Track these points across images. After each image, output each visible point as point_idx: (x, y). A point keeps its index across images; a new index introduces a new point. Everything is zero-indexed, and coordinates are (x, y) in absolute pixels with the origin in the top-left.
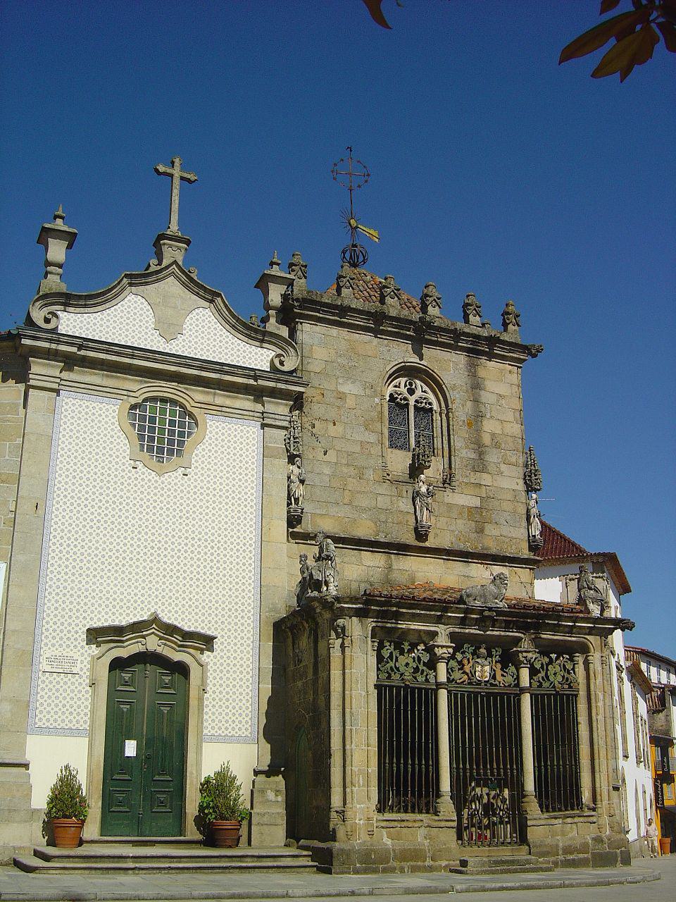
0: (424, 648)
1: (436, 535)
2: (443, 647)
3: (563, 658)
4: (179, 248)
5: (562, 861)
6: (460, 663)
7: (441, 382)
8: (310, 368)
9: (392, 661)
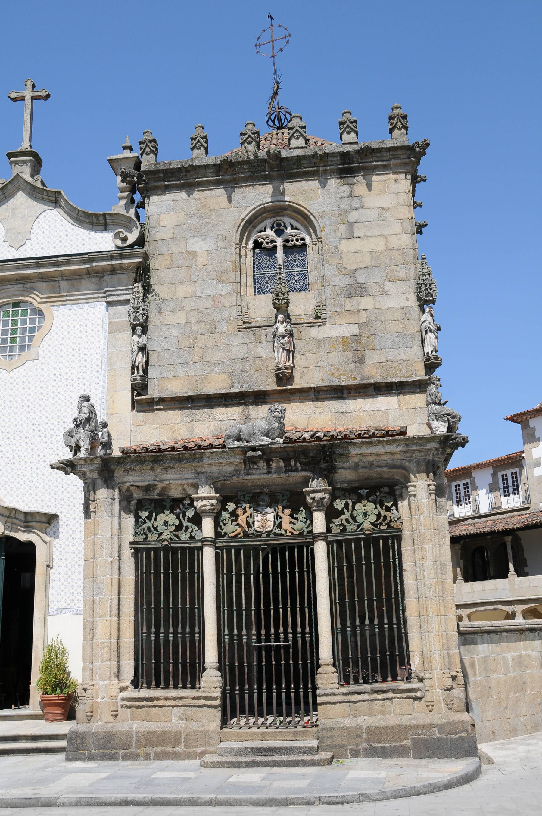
0: (189, 502)
1: (303, 374)
2: (202, 499)
3: (380, 492)
4: (25, 162)
5: (365, 749)
6: (234, 514)
7: (307, 213)
8: (158, 236)
9: (151, 521)
